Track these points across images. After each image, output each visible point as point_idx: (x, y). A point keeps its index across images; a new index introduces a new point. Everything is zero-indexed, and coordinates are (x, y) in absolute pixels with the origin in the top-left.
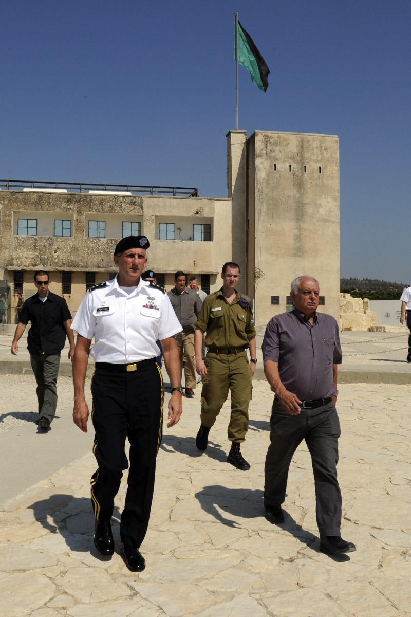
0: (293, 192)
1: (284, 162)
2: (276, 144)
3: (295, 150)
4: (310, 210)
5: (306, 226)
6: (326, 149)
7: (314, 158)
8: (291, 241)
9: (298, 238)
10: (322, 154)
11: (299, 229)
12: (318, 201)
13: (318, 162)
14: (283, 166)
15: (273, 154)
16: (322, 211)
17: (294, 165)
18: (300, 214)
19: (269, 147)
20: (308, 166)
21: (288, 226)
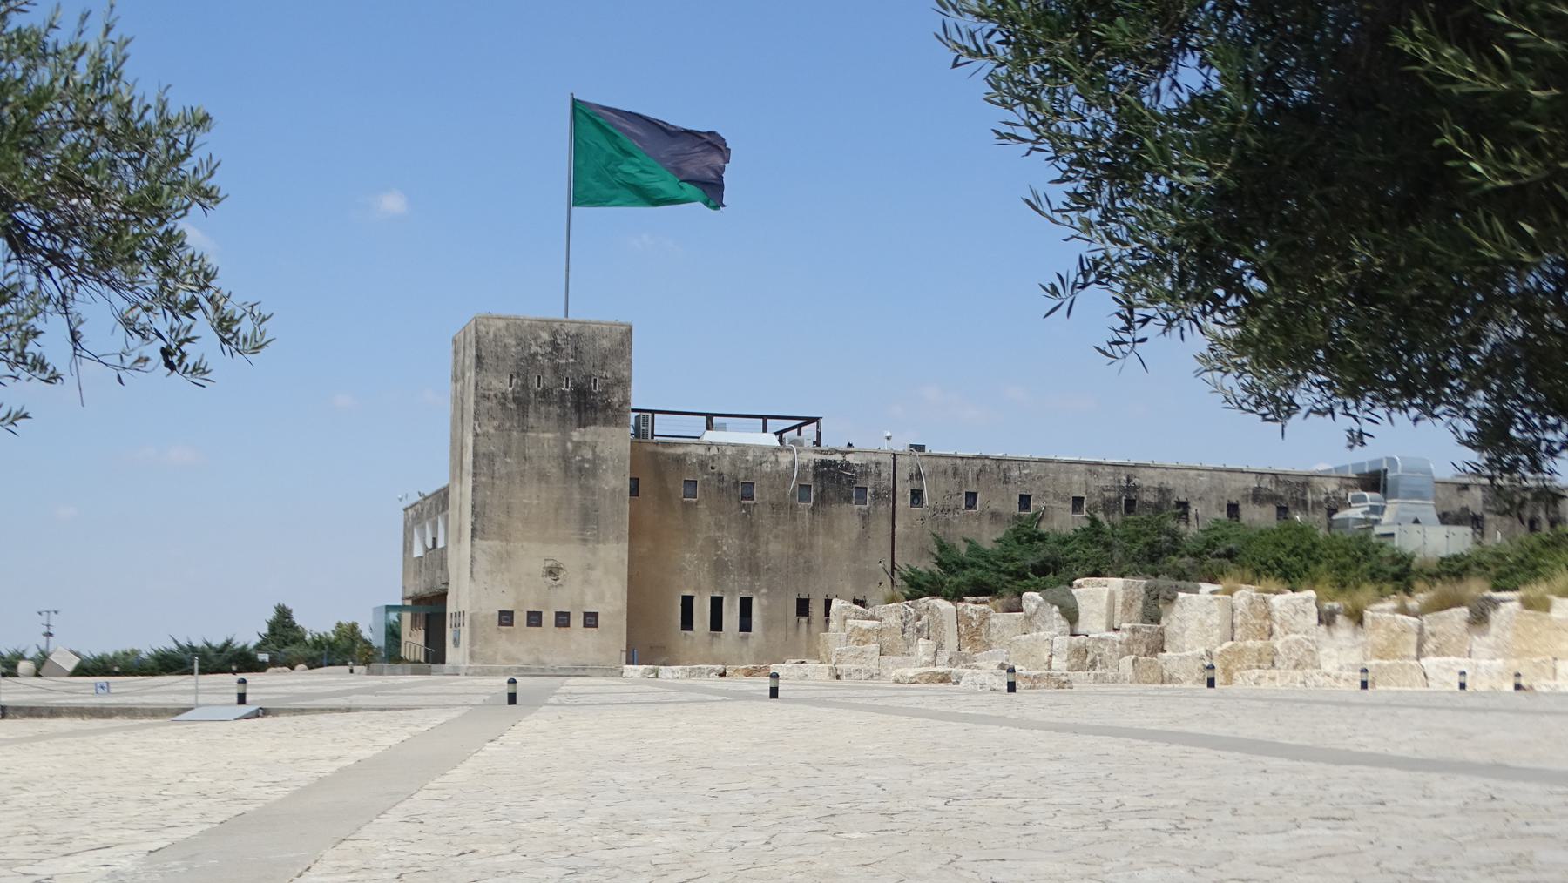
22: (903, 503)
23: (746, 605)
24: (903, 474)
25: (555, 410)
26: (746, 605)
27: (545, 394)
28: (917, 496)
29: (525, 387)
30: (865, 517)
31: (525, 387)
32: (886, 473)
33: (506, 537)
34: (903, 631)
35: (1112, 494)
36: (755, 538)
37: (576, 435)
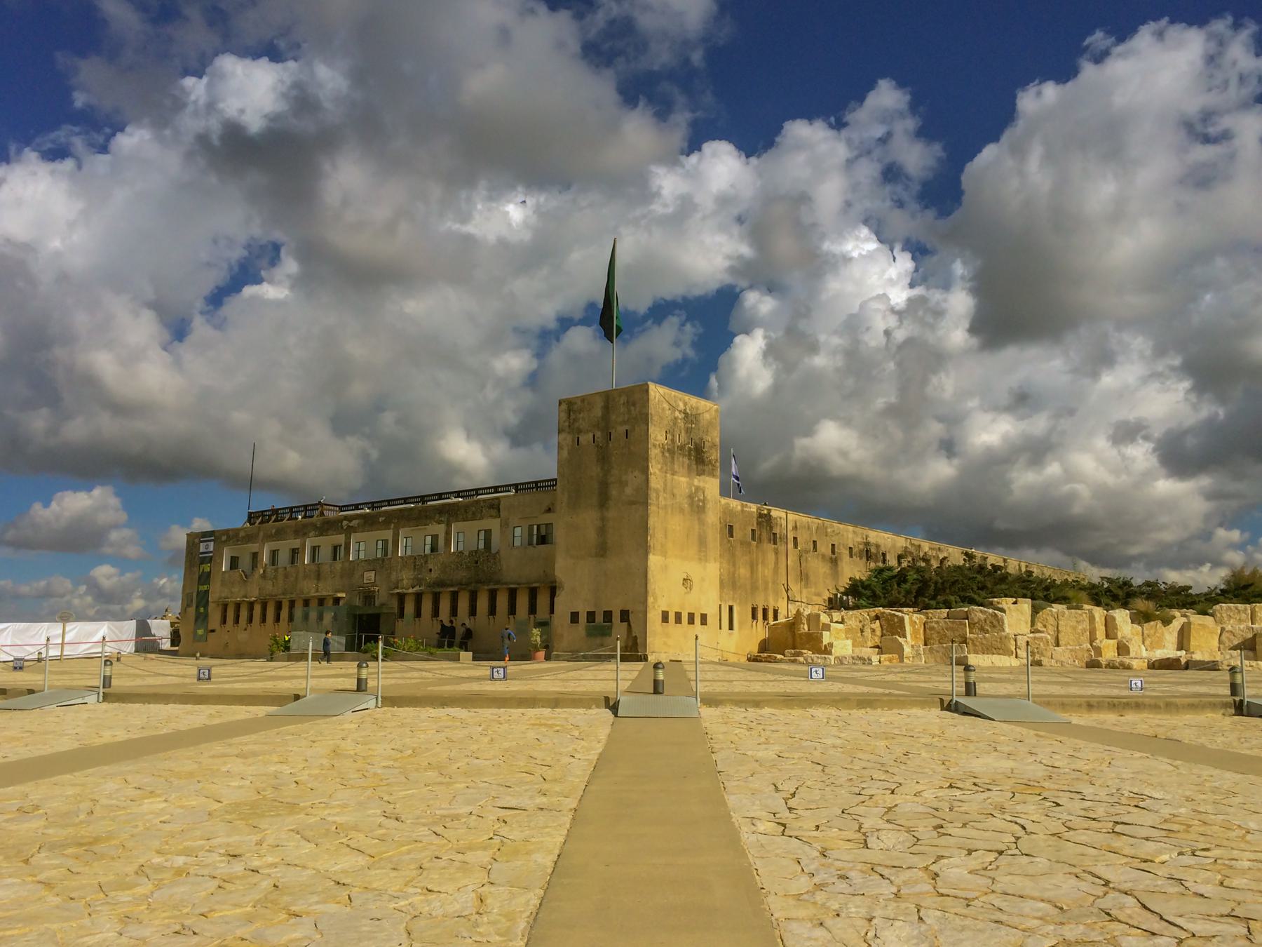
0: (595, 470)
1: (588, 431)
2: (580, 411)
3: (600, 414)
4: (614, 492)
5: (611, 513)
6: (634, 405)
7: (620, 419)
8: (592, 535)
9: (602, 531)
10: (629, 411)
11: (603, 519)
12: (624, 478)
13: (624, 423)
14: (586, 439)
15: (576, 425)
16: (628, 491)
17: (598, 434)
18: (604, 500)
19: (573, 416)
20: (613, 431)
21: (588, 518)
22: (791, 545)
23: (731, 608)
24: (790, 527)
25: (686, 461)
26: (731, 608)
27: (681, 448)
28: (795, 538)
29: (673, 440)
30: (776, 552)
31: (673, 440)
32: (784, 523)
33: (664, 554)
34: (862, 631)
35: (861, 547)
36: (734, 565)
37: (696, 482)
